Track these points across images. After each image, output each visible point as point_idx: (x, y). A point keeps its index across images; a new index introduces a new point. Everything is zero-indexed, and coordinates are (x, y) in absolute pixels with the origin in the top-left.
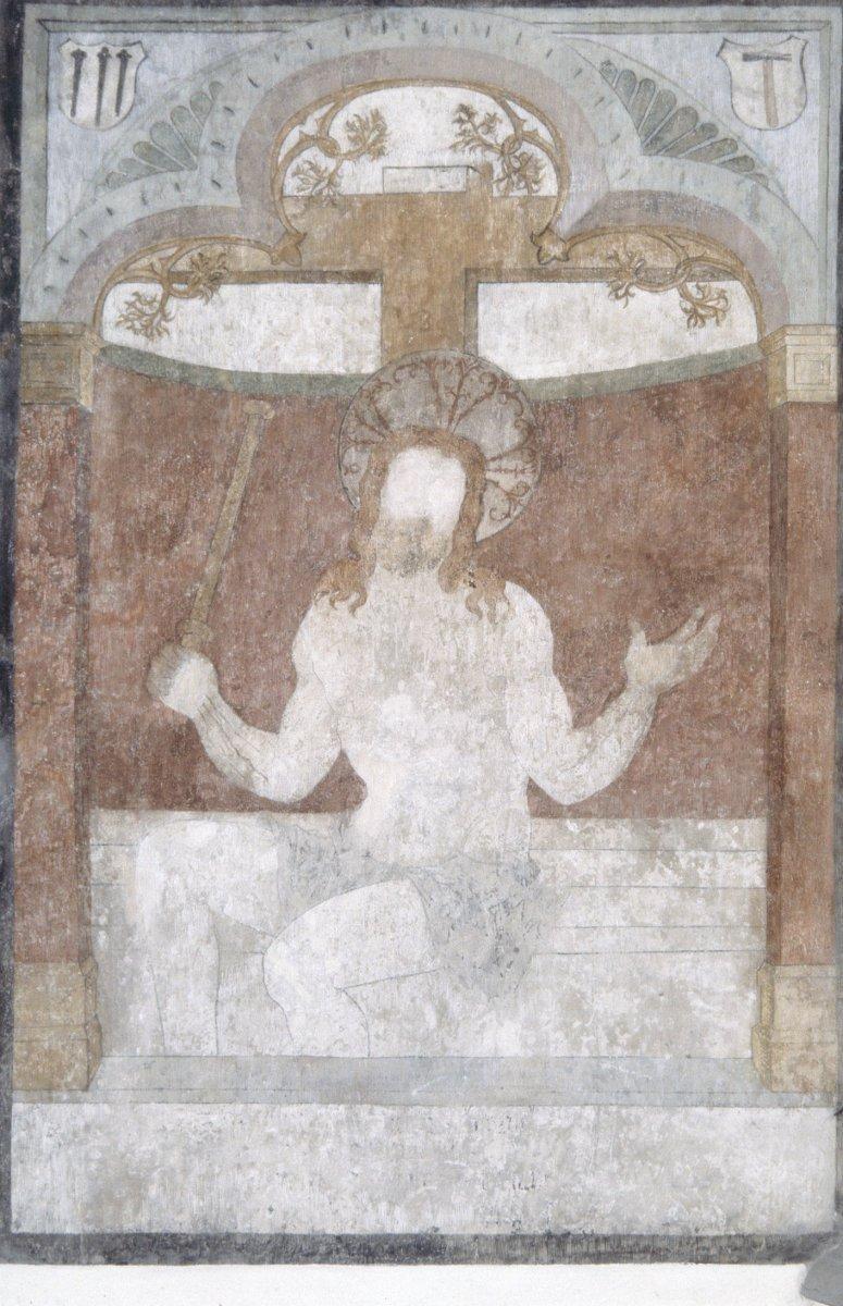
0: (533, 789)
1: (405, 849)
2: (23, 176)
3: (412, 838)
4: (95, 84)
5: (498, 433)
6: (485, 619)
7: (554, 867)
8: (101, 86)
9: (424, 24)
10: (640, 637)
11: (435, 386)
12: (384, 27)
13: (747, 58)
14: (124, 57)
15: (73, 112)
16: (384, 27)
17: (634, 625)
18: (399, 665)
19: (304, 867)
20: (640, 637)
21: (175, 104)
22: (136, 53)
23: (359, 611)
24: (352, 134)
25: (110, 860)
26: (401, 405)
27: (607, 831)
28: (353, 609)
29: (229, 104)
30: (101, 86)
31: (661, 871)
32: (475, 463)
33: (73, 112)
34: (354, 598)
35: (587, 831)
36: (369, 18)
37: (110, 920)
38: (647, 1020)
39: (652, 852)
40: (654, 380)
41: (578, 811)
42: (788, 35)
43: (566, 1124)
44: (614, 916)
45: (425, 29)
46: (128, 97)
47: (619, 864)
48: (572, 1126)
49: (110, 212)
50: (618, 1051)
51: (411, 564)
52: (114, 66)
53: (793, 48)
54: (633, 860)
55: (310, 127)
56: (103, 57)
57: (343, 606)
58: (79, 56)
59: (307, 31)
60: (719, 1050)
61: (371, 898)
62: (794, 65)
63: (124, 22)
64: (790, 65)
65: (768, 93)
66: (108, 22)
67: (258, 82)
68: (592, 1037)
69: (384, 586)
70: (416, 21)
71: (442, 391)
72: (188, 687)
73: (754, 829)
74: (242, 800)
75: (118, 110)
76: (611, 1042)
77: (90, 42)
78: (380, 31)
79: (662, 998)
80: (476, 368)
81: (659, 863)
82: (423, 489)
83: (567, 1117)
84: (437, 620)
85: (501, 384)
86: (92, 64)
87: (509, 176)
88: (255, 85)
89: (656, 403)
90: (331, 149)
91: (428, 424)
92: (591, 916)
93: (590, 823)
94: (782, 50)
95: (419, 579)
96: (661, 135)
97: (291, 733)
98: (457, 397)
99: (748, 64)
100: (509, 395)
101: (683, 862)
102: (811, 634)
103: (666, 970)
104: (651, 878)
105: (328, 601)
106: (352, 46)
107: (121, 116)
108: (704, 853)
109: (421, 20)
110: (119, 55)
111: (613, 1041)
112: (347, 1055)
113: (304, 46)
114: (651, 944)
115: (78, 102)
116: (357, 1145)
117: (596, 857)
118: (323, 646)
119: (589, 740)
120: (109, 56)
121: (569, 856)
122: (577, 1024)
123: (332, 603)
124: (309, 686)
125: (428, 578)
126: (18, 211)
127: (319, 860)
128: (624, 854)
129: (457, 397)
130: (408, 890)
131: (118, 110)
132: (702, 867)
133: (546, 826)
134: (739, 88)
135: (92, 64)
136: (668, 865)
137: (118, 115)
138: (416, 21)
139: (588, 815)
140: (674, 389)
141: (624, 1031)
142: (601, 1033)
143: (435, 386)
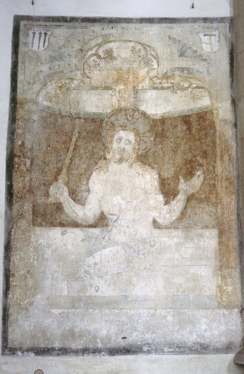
0: (154, 222)
1: (120, 237)
2: (19, 62)
3: (121, 235)
4: (38, 40)
5: (143, 127)
6: (141, 176)
7: (161, 243)
8: (40, 40)
9: (123, 27)
10: (182, 180)
11: (126, 115)
12: (112, 28)
13: (205, 35)
14: (46, 34)
15: (32, 47)
16: (112, 28)
17: (180, 177)
18: (117, 188)
19: (91, 243)
20: (182, 180)
21: (59, 45)
22: (49, 33)
23: (107, 173)
24: (104, 53)
25: (38, 241)
26: (118, 120)
27: (175, 232)
28: (105, 173)
29: (73, 45)
30: (40, 40)
31: (190, 243)
32: (137, 134)
33: (32, 47)
34: (105, 170)
35: (169, 232)
36: (108, 26)
37: (38, 258)
38: (187, 285)
39: (187, 238)
40: (184, 114)
41: (166, 228)
42: (214, 30)
43: (166, 314)
44: (177, 256)
45: (123, 28)
46: (46, 44)
47: (178, 241)
48: (167, 315)
49: (41, 71)
50: (179, 294)
51: (120, 161)
52: (43, 36)
53: (217, 33)
54: (182, 240)
55: (93, 52)
56: (40, 34)
57: (102, 173)
58: (34, 33)
59: (92, 28)
60: (208, 293)
61: (111, 251)
62: (217, 37)
63: (46, 25)
64: (216, 37)
65: (211, 43)
66: (42, 25)
67: (80, 41)
68: (172, 290)
69: (113, 167)
70: (121, 26)
71: (128, 116)
72: (60, 192)
73: (214, 232)
74: (76, 225)
75: (44, 47)
76: (177, 290)
77: (37, 30)
78: (111, 29)
79: (191, 278)
80: (138, 111)
81: (189, 241)
82: (124, 140)
83: (166, 312)
84: (128, 176)
85: (144, 114)
86: (37, 35)
87: (145, 64)
88: (79, 41)
89: (185, 120)
90: (99, 57)
91: (125, 125)
92: (171, 256)
93: (170, 230)
94: (214, 33)
95: (123, 165)
96: (184, 53)
97: (88, 207)
98: (133, 118)
99: (205, 37)
100: (146, 117)
101: (196, 241)
102: (228, 179)
103: (192, 270)
104: (187, 245)
105: (98, 171)
106: (104, 32)
107: (45, 48)
108: (201, 238)
109: (122, 26)
110: (44, 33)
111: (178, 290)
112: (104, 295)
113: (92, 32)
114: (188, 263)
115: (34, 45)
116: (107, 321)
117: (172, 239)
118: (98, 183)
119: (169, 208)
120: (42, 33)
121: (165, 239)
122: (168, 286)
123: (99, 171)
124: (93, 194)
125: (125, 165)
126: (17, 71)
127: (96, 241)
128: (179, 239)
129: (133, 118)
130: (120, 248)
131: (44, 47)
132: (201, 242)
133: (158, 231)
134: (203, 43)
135: (37, 35)
136: (192, 242)
137: (44, 47)
138: (121, 26)
139: (169, 228)
140: (189, 116)
141: (181, 288)
142: (174, 288)
143: (126, 115)
